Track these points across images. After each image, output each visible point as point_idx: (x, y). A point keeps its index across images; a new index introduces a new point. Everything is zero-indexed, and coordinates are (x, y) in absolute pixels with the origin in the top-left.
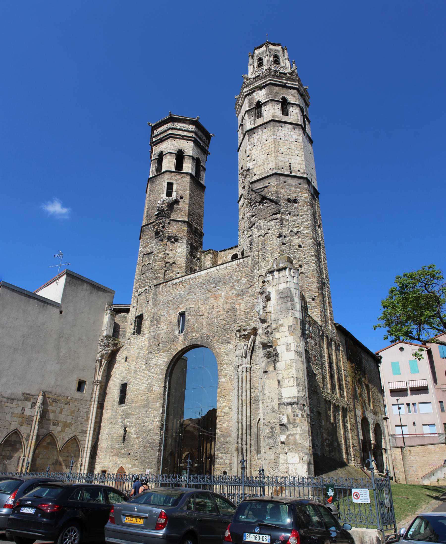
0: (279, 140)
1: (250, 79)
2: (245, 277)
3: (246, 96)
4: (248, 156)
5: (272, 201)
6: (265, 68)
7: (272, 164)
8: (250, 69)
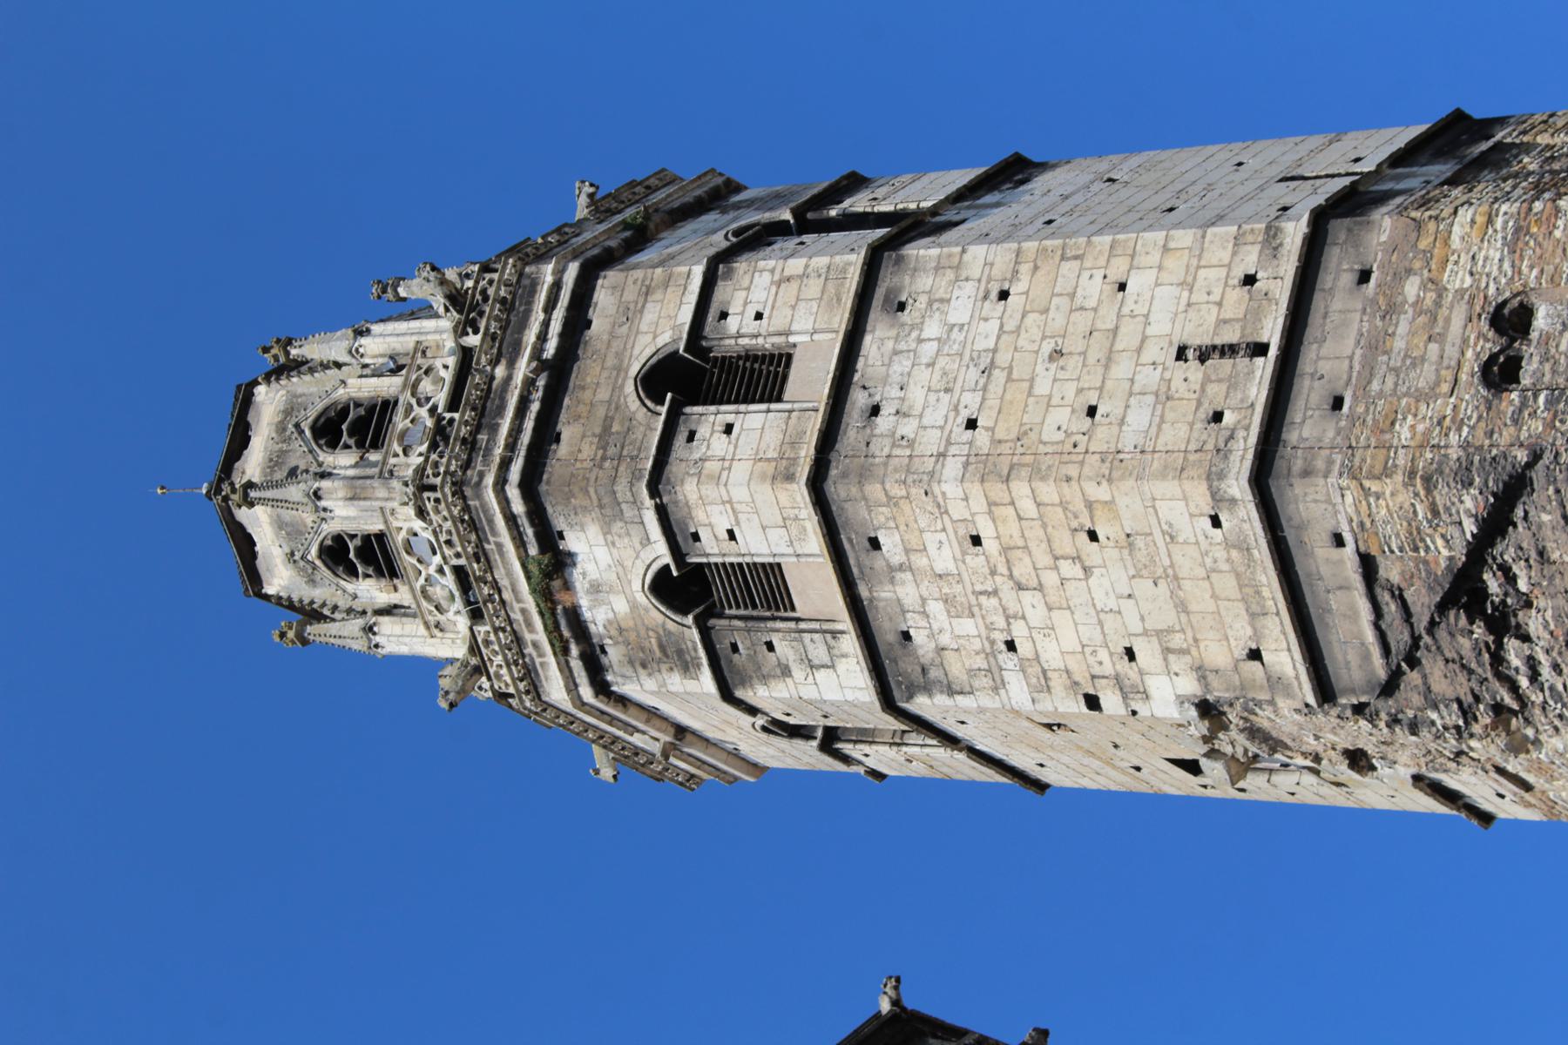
0: (981, 437)
1: (474, 649)
3: (601, 687)
4: (1093, 702)
5: (1495, 524)
6: (405, 521)
7: (1179, 506)
8: (398, 638)
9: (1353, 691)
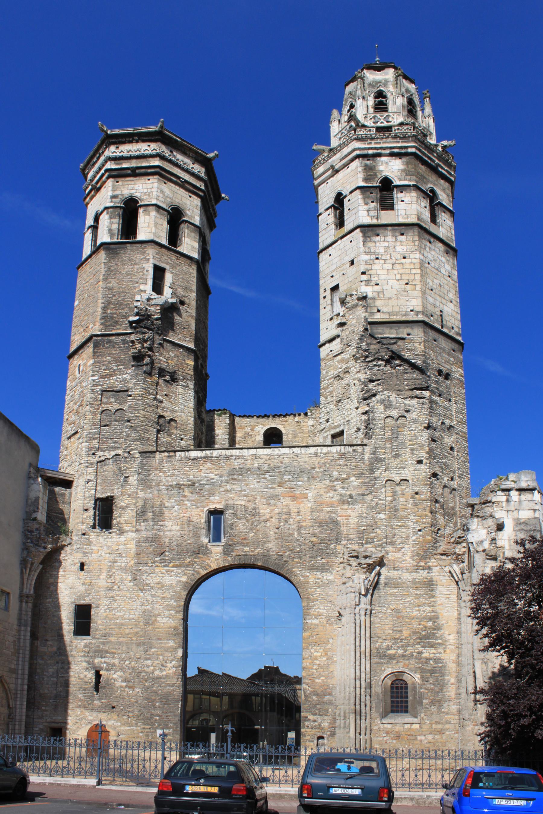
2: (358, 477)
4: (363, 273)
9: (371, 329)
